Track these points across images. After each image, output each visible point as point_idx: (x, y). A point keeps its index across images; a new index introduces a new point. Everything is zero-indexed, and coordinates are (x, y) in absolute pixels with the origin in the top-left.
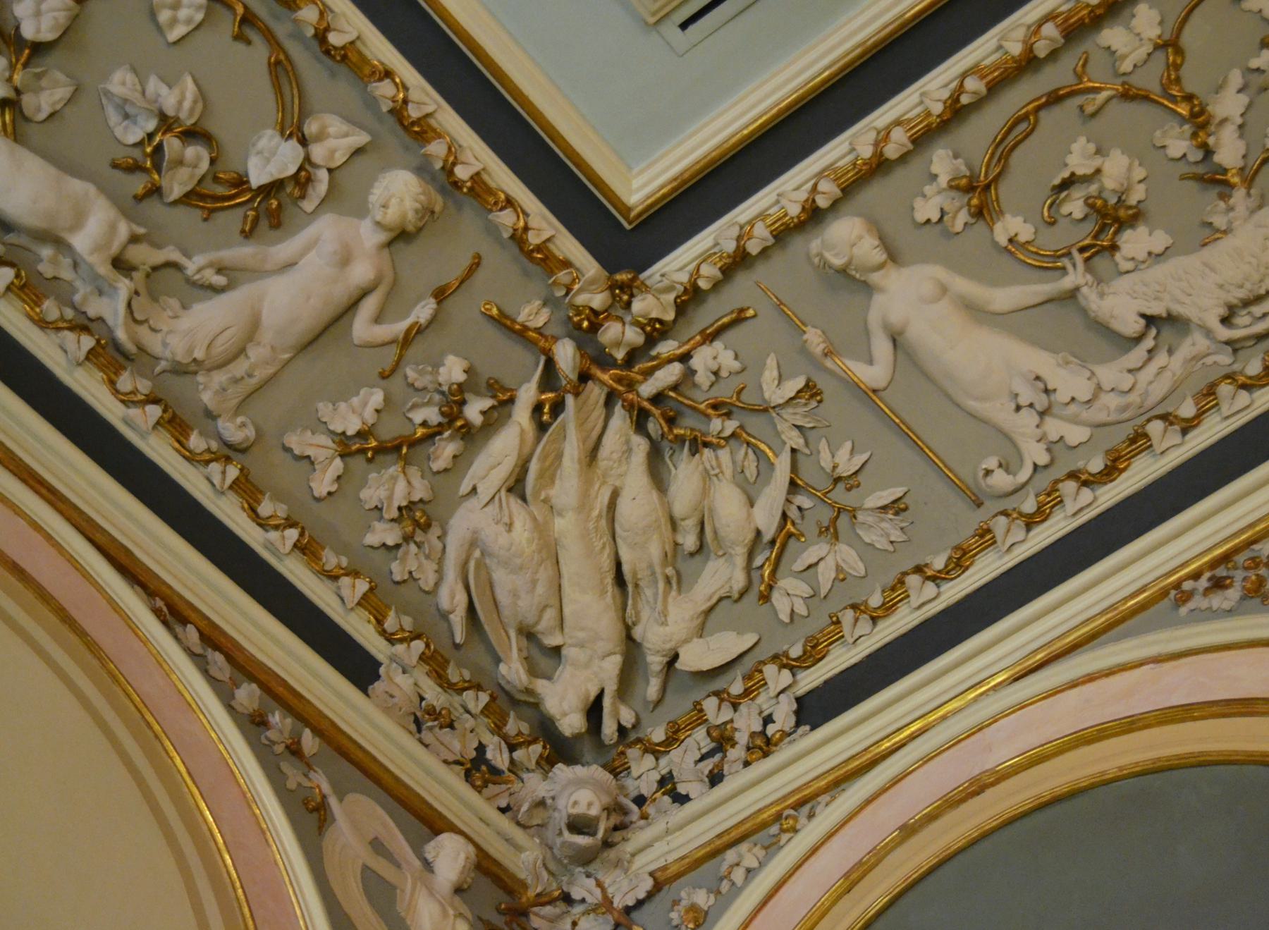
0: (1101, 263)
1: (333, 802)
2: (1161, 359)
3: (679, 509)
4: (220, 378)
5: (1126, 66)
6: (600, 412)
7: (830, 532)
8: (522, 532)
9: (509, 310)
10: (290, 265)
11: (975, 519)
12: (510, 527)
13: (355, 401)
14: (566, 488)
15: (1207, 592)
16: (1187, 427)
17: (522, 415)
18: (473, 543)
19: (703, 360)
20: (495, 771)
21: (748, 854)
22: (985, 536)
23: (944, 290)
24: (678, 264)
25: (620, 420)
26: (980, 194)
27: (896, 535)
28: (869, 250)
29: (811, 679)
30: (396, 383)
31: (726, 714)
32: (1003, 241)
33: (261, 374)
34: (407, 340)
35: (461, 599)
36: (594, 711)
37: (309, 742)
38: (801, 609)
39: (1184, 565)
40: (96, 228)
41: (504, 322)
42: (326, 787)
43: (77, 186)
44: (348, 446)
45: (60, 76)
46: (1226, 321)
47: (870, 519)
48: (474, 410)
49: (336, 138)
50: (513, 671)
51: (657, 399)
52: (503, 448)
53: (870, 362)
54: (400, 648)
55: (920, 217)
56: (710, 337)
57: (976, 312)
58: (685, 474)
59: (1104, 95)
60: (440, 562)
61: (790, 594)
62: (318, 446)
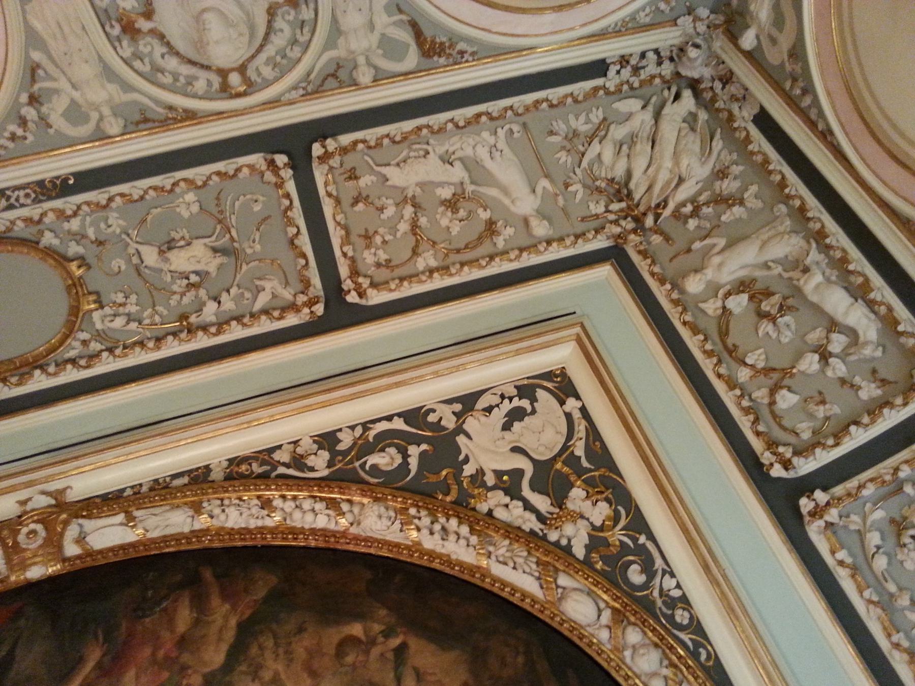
0: (459, 191)
1: (786, 58)
2: (451, 150)
3: (626, 159)
4: (781, 229)
5: (431, 252)
6: (643, 201)
7: (576, 133)
8: (684, 162)
9: (664, 242)
10: (742, 268)
11: (526, 118)
12: (688, 165)
13: (732, 218)
14: (663, 177)
15: (466, 52)
16: (452, 120)
17: (671, 206)
18: (703, 163)
19: (601, 209)
20: (721, 80)
21: (643, 19)
22: (527, 109)
23: (513, 202)
24: (600, 243)
25: (637, 196)
26: (491, 228)
27: (554, 123)
28: (534, 222)
29: (599, 82)
30: (715, 222)
31: (632, 79)
32: (488, 210)
33: (764, 230)
34: (705, 238)
35: (714, 144)
36: (677, 97)
37: (787, 85)
38: (594, 109)
39: (470, 66)
40: (812, 284)
41: (667, 239)
42: (787, 64)
43: (814, 298)
44: (741, 202)
45: (810, 342)
46: (427, 153)
47: (561, 133)
48: (689, 208)
49: (712, 307)
50: (703, 116)
51: (621, 201)
52: (684, 193)
53: (544, 188)
54: (743, 125)
55: (513, 229)
56: (597, 216)
57: (505, 191)
58: (619, 172)
59: (442, 245)
60: (718, 159)
61: (597, 116)
62: (753, 203)
